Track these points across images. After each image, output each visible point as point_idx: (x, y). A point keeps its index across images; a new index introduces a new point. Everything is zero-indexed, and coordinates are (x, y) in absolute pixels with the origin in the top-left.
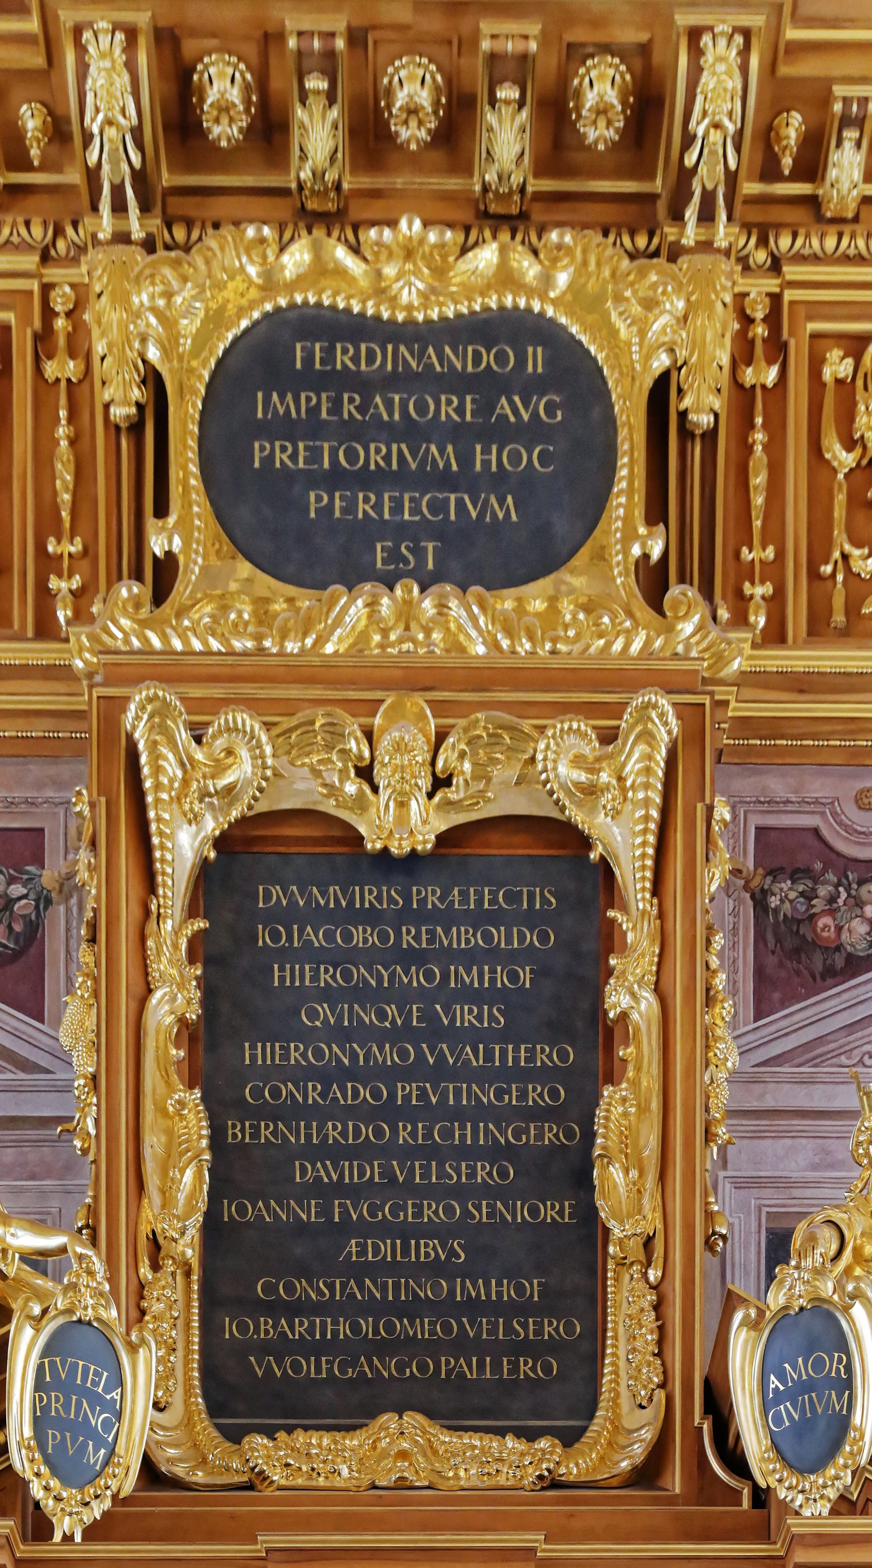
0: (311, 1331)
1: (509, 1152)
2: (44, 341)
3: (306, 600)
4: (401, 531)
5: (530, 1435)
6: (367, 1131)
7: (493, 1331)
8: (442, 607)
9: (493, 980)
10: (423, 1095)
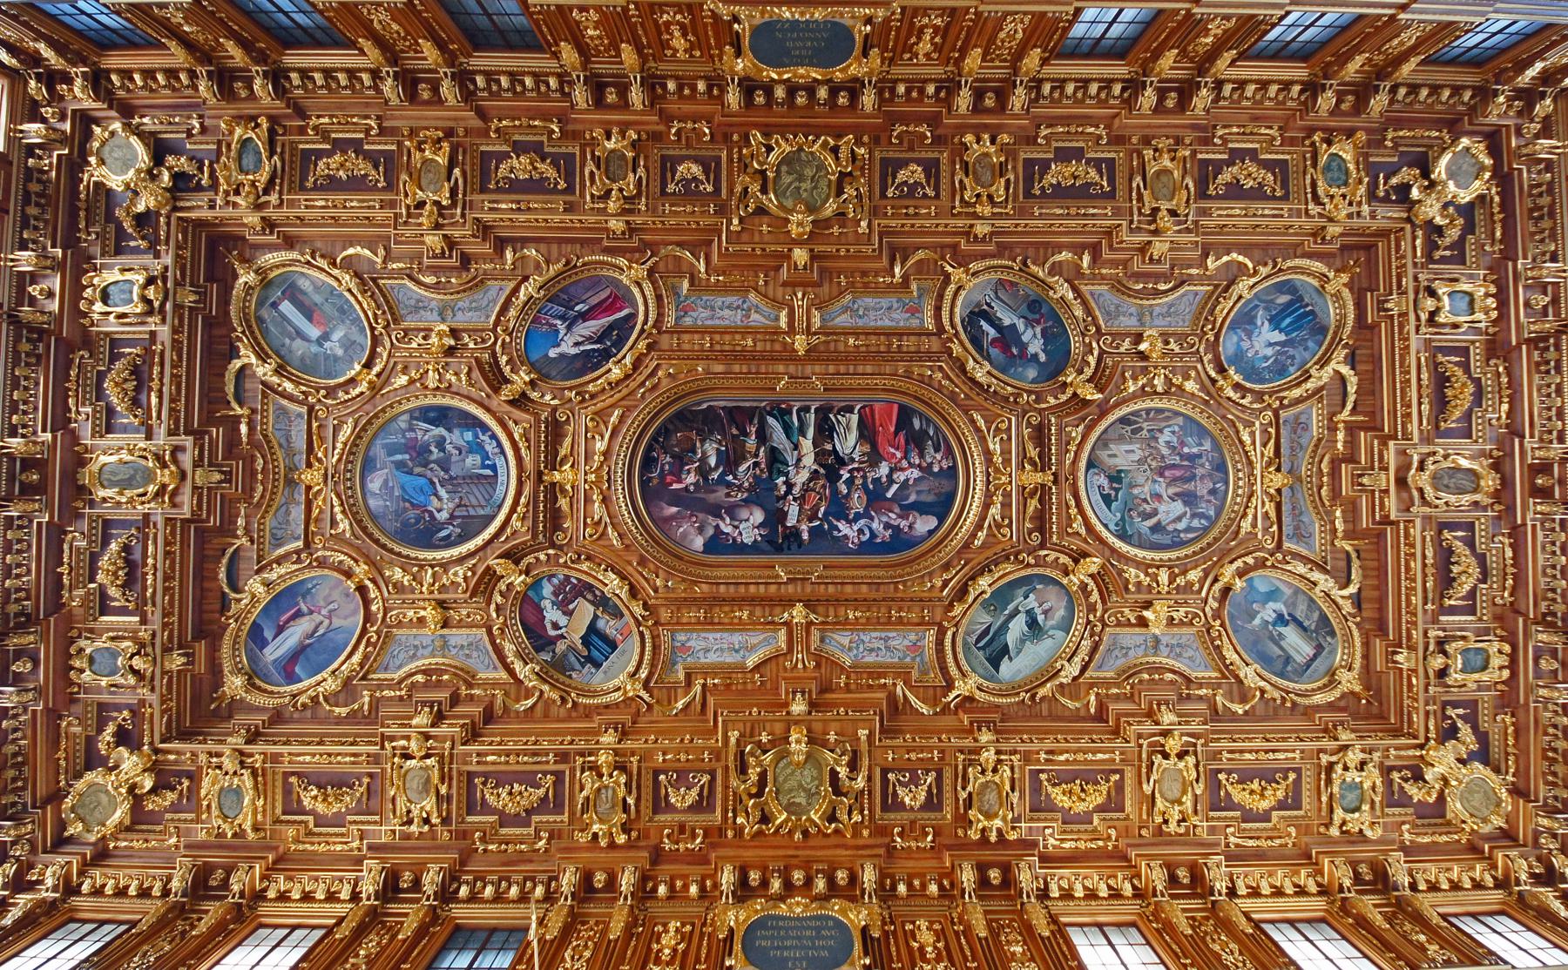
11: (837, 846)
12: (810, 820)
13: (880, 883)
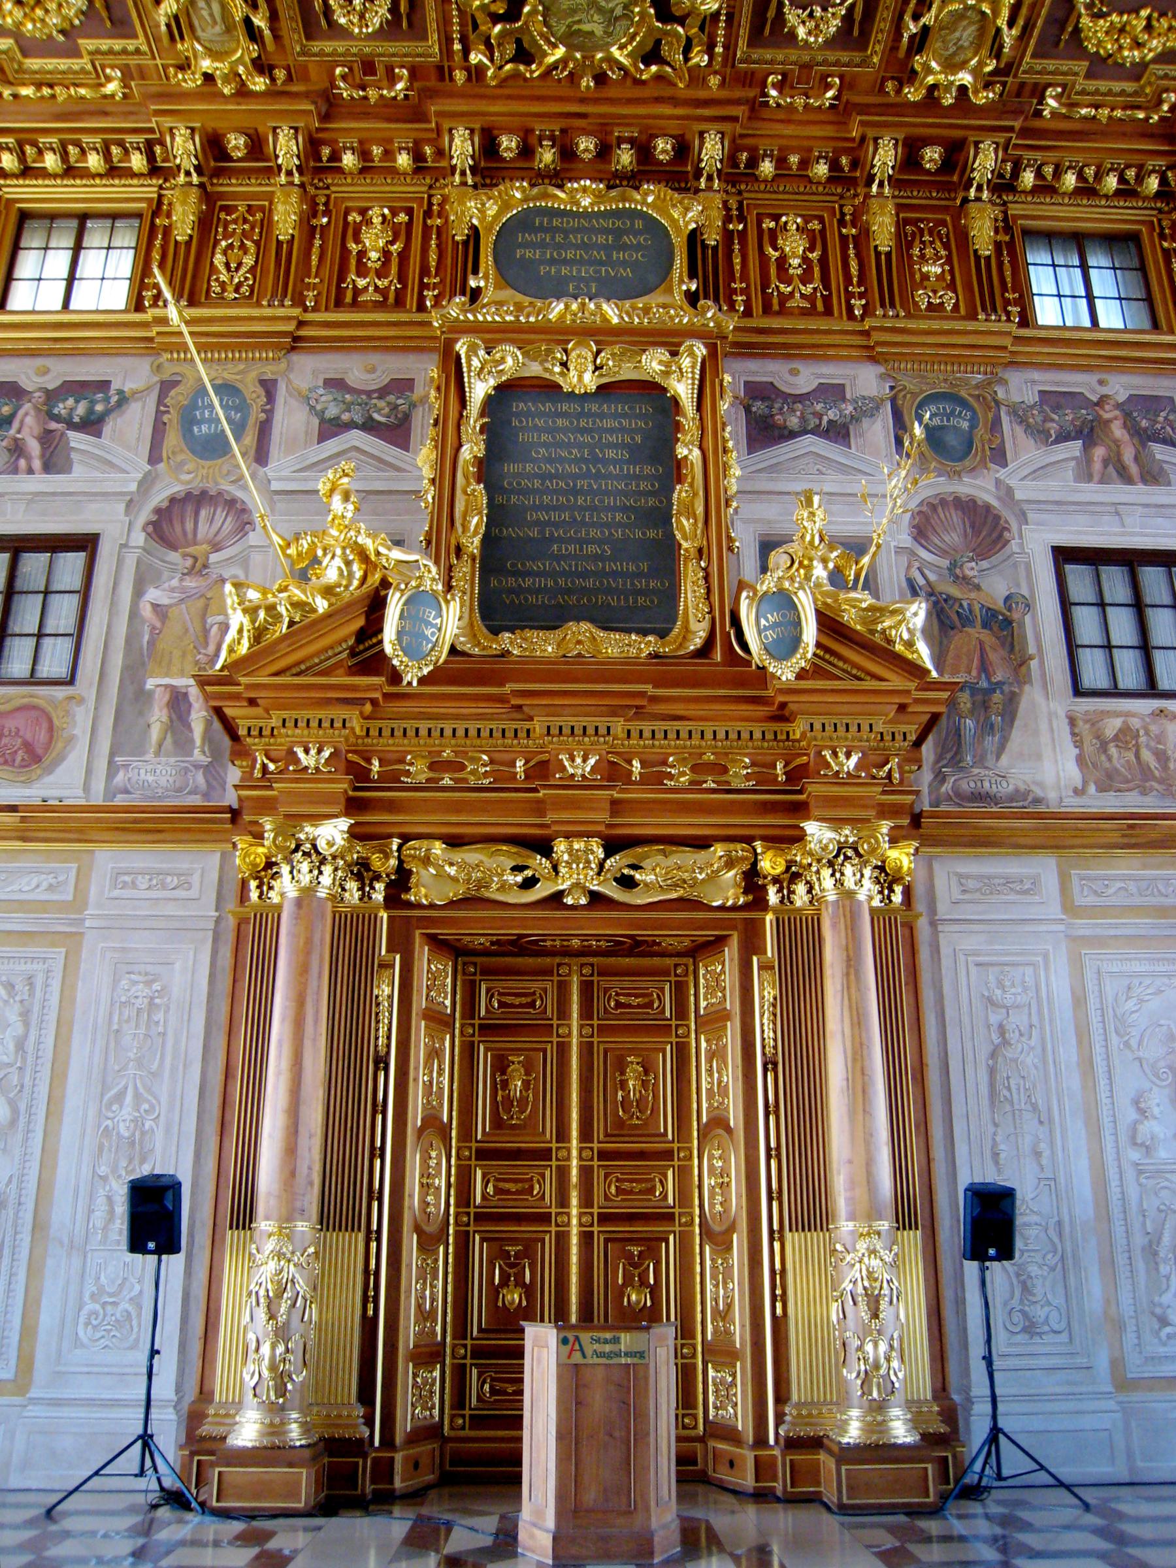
2: (428, 214)
4: (582, 279)
5: (644, 633)
6: (562, 499)
7: (624, 584)
8: (598, 307)
10: (590, 485)
11: (658, 100)
12: (610, 59)
13: (731, 159)
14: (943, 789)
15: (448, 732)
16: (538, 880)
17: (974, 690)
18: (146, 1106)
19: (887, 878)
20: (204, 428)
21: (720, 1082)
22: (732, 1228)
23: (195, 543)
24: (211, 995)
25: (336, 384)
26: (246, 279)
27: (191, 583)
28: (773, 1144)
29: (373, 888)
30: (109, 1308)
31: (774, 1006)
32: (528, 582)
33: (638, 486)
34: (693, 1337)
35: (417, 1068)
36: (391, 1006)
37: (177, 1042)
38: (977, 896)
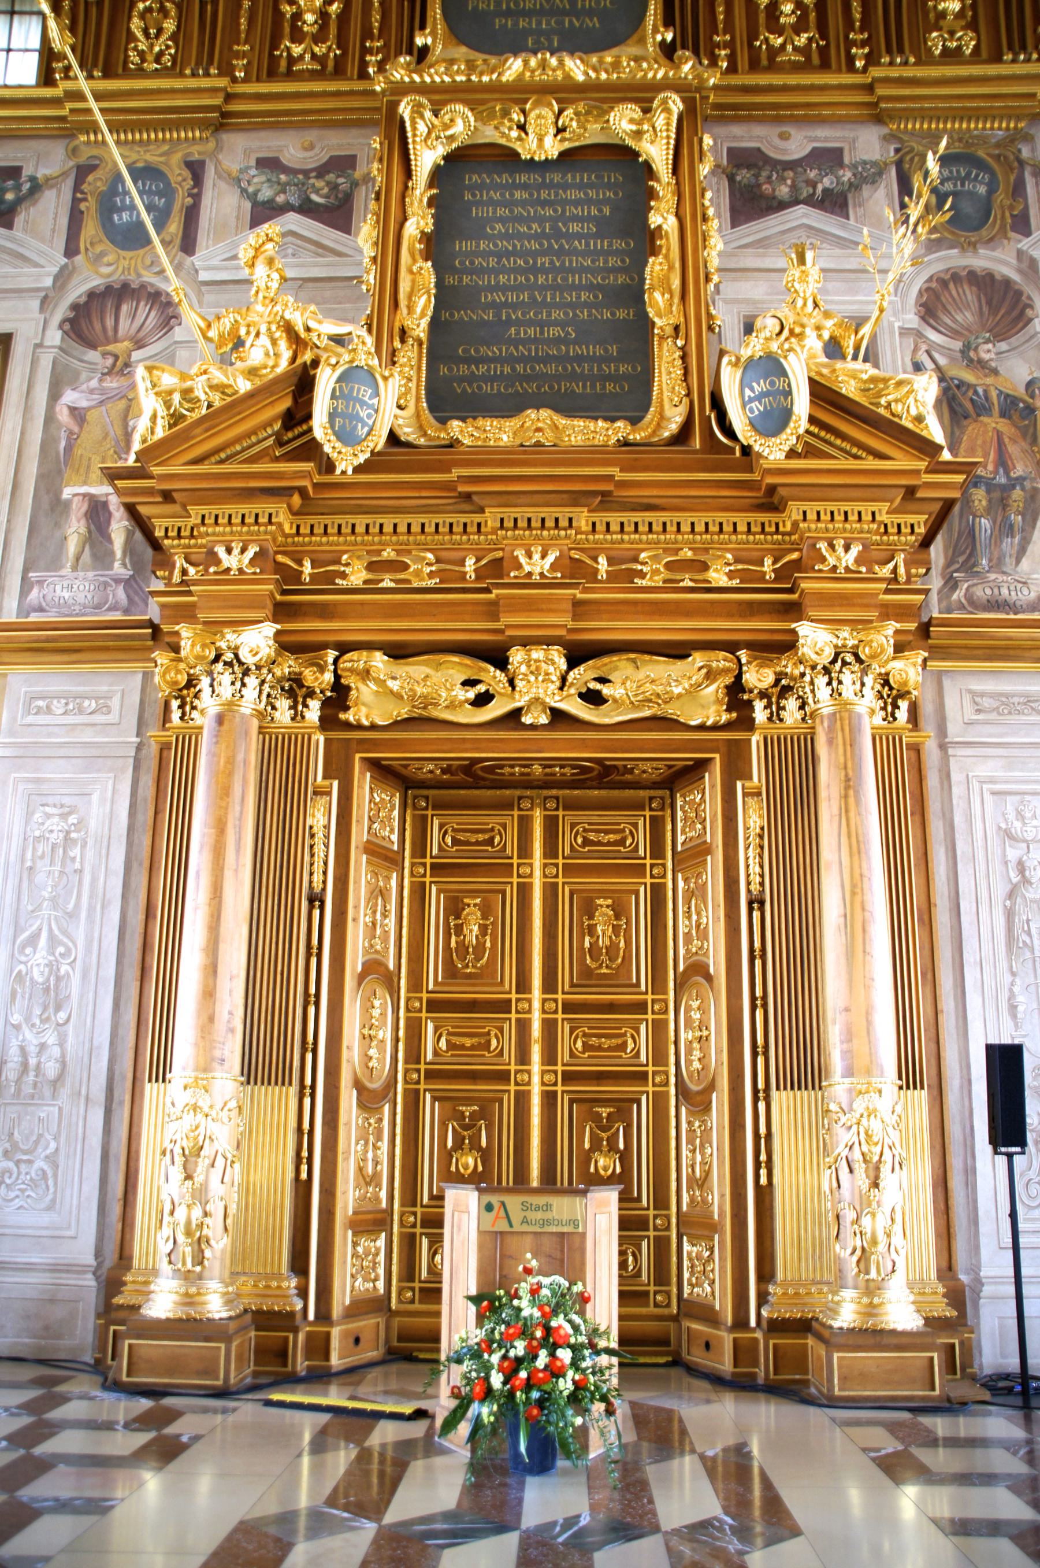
0: (488, 370)
1: (599, 287)
3: (493, 60)
7: (591, 369)
9: (589, 212)
10: (552, 262)
14: (955, 597)
15: (388, 528)
16: (492, 697)
17: (990, 487)
18: (61, 949)
19: (892, 694)
20: (125, 216)
21: (698, 926)
22: (712, 1087)
23: (116, 340)
24: (131, 829)
25: (269, 164)
26: (168, 47)
27: (112, 384)
28: (759, 993)
29: (305, 706)
30: (23, 1167)
31: (761, 837)
32: (483, 369)
33: (606, 262)
34: (667, 1207)
35: (356, 907)
36: (327, 837)
37: (94, 880)
38: (993, 716)
